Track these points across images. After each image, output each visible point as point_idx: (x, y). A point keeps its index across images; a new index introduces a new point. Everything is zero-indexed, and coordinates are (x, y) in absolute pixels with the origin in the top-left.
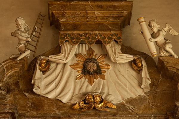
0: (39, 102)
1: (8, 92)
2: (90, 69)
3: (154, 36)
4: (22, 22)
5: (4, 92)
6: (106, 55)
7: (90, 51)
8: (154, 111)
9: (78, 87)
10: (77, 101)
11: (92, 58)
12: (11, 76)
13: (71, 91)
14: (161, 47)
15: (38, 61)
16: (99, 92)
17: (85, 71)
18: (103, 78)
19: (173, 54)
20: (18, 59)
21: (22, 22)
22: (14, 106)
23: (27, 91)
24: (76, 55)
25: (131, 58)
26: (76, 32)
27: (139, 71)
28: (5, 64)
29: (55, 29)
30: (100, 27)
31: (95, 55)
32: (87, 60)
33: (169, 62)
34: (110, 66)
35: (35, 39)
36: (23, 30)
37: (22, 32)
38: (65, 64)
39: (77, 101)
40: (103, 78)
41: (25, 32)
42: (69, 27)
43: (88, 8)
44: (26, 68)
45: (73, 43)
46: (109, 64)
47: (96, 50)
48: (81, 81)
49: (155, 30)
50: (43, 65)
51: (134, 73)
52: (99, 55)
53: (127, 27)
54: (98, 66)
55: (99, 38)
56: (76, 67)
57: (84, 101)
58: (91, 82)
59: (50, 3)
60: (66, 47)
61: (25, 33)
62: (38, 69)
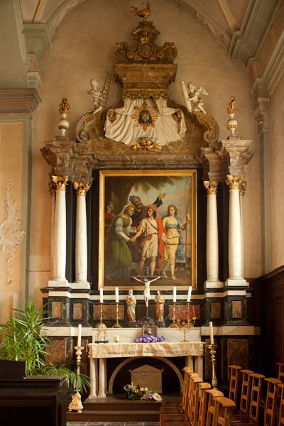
0: (109, 144)
1: (88, 139)
2: (145, 119)
3: (191, 95)
4: (95, 84)
5: (86, 139)
6: (156, 108)
7: (145, 104)
8: (187, 151)
10: (136, 143)
12: (89, 126)
13: (131, 136)
14: (195, 105)
15: (108, 113)
17: (141, 121)
18: (154, 126)
21: (95, 84)
22: (93, 148)
23: (101, 136)
24: (135, 108)
25: (173, 111)
26: (134, 90)
27: (179, 121)
29: (120, 88)
30: (153, 85)
35: (105, 96)
36: (96, 89)
37: (96, 91)
38: (126, 116)
39: (136, 143)
40: (154, 126)
42: (129, 85)
43: (143, 69)
44: (99, 118)
45: (133, 99)
46: (158, 115)
47: (149, 102)
49: (192, 91)
51: (175, 122)
54: (150, 117)
55: (151, 94)
57: (140, 144)
58: (145, 130)
59: (115, 65)
60: (128, 101)
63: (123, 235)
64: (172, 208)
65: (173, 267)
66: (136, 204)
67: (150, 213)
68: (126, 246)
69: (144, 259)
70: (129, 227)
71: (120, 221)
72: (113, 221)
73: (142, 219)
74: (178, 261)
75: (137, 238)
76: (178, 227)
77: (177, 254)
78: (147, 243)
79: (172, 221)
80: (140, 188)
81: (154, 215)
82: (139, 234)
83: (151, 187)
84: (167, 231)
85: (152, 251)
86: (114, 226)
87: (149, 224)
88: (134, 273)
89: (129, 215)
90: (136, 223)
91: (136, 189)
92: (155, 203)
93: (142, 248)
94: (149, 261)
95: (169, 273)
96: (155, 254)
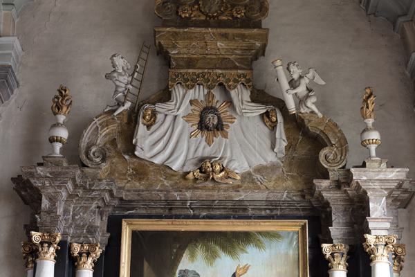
0: (142, 170)
2: (209, 123)
3: (293, 84)
6: (230, 102)
9: (192, 149)
11: (212, 108)
14: (301, 101)
16: (220, 156)
17: (202, 126)
19: (316, 111)
20: (116, 114)
24: (191, 102)
26: (191, 71)
27: (273, 127)
28: (99, 120)
29: (163, 71)
31: (215, 101)
32: (205, 109)
33: (311, 121)
34: (235, 118)
37: (120, 74)
41: (123, 74)
45: (189, 87)
47: (217, 94)
48: (197, 141)
49: (296, 76)
50: (147, 117)
51: (266, 130)
52: (222, 102)
53: (261, 59)
54: (219, 118)
55: (221, 79)
56: (190, 119)
57: (200, 169)
59: (156, 30)
60: (178, 92)
61: (123, 76)
62: (140, 123)
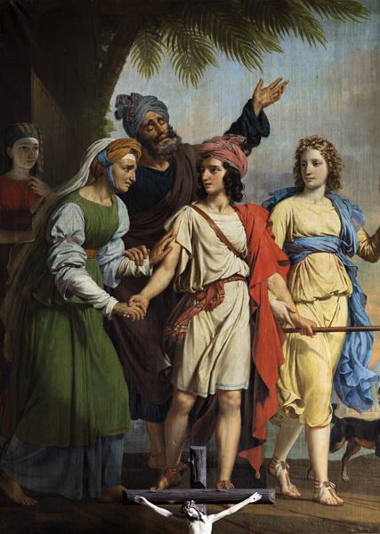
63: (89, 286)
64: (316, 154)
65: (322, 439)
66: (148, 131)
67: (215, 179)
68: (101, 339)
69: (187, 401)
70: (116, 248)
71: (71, 220)
72: (36, 221)
73: (172, 210)
74: (347, 412)
75: (154, 302)
76: (344, 245)
77: (339, 377)
78: (202, 326)
79: (314, 215)
80: (166, 56)
81: (233, 187)
82: (161, 279)
83: (219, 54)
84: (293, 262)
85: (221, 364)
86: (46, 245)
87: (211, 232)
88: (141, 471)
89: (113, 190)
90: (149, 229)
91: (148, 62)
92: (236, 128)
93: (175, 350)
94: (208, 411)
95: (303, 470)
96: (237, 379)
